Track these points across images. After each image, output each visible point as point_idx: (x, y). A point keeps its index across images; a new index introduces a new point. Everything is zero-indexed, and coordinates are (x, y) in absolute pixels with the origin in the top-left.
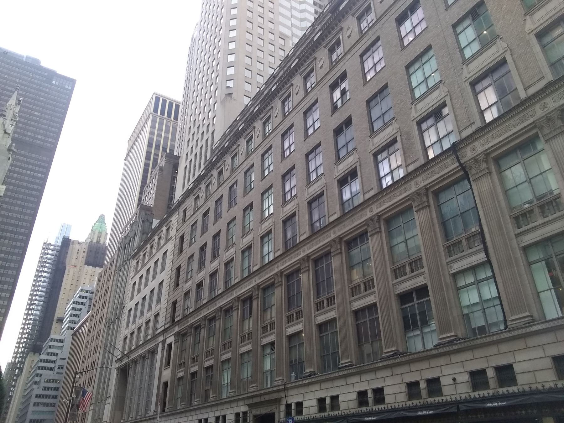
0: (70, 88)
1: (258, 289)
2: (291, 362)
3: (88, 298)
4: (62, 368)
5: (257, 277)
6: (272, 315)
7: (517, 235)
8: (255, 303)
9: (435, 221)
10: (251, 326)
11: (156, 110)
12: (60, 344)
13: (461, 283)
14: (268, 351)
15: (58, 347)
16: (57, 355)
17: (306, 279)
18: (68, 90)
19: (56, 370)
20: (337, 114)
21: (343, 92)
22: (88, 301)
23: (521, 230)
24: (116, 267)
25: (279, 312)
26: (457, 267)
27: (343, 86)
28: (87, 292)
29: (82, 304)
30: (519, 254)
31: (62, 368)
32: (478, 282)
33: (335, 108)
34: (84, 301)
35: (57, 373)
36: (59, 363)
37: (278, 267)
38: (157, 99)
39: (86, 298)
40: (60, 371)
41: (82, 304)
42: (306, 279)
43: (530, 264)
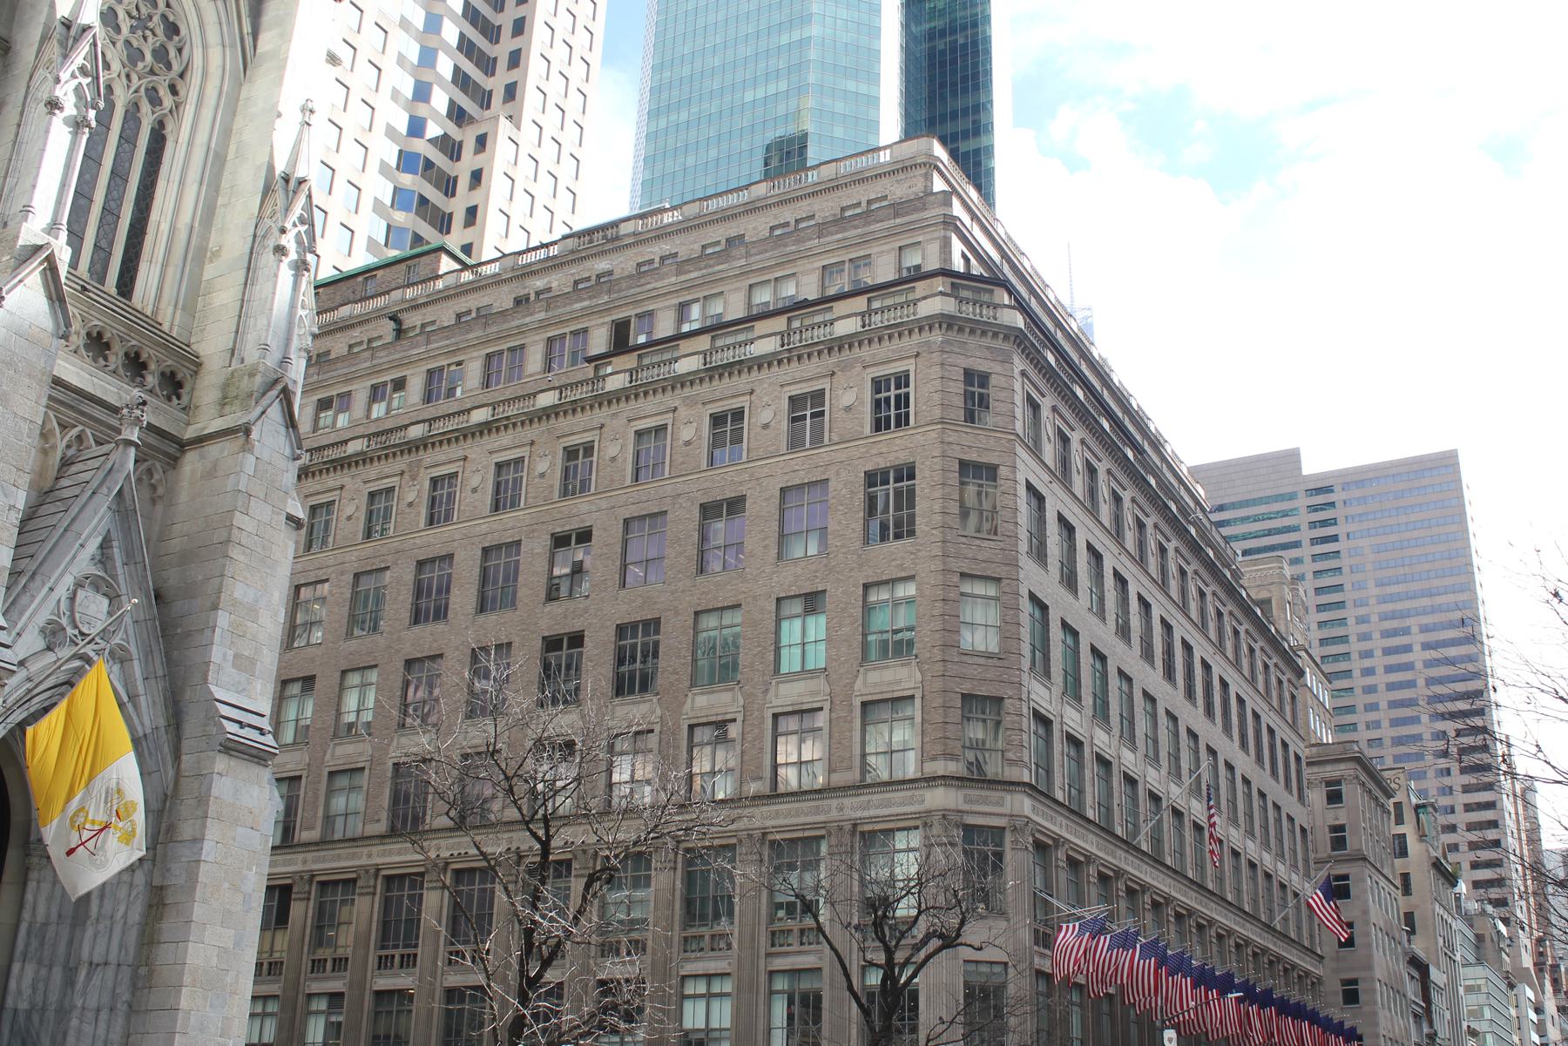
1: (311, 880)
2: (376, 1037)
5: (309, 856)
6: (346, 940)
7: (768, 955)
8: (297, 909)
9: (678, 894)
10: (277, 947)
13: (689, 990)
14: (323, 1005)
17: (434, 904)
20: (554, 608)
21: (578, 569)
23: (774, 950)
25: (362, 941)
26: (689, 968)
27: (579, 556)
30: (763, 978)
32: (709, 996)
33: (552, 595)
37: (370, 856)
42: (434, 904)
43: (771, 993)
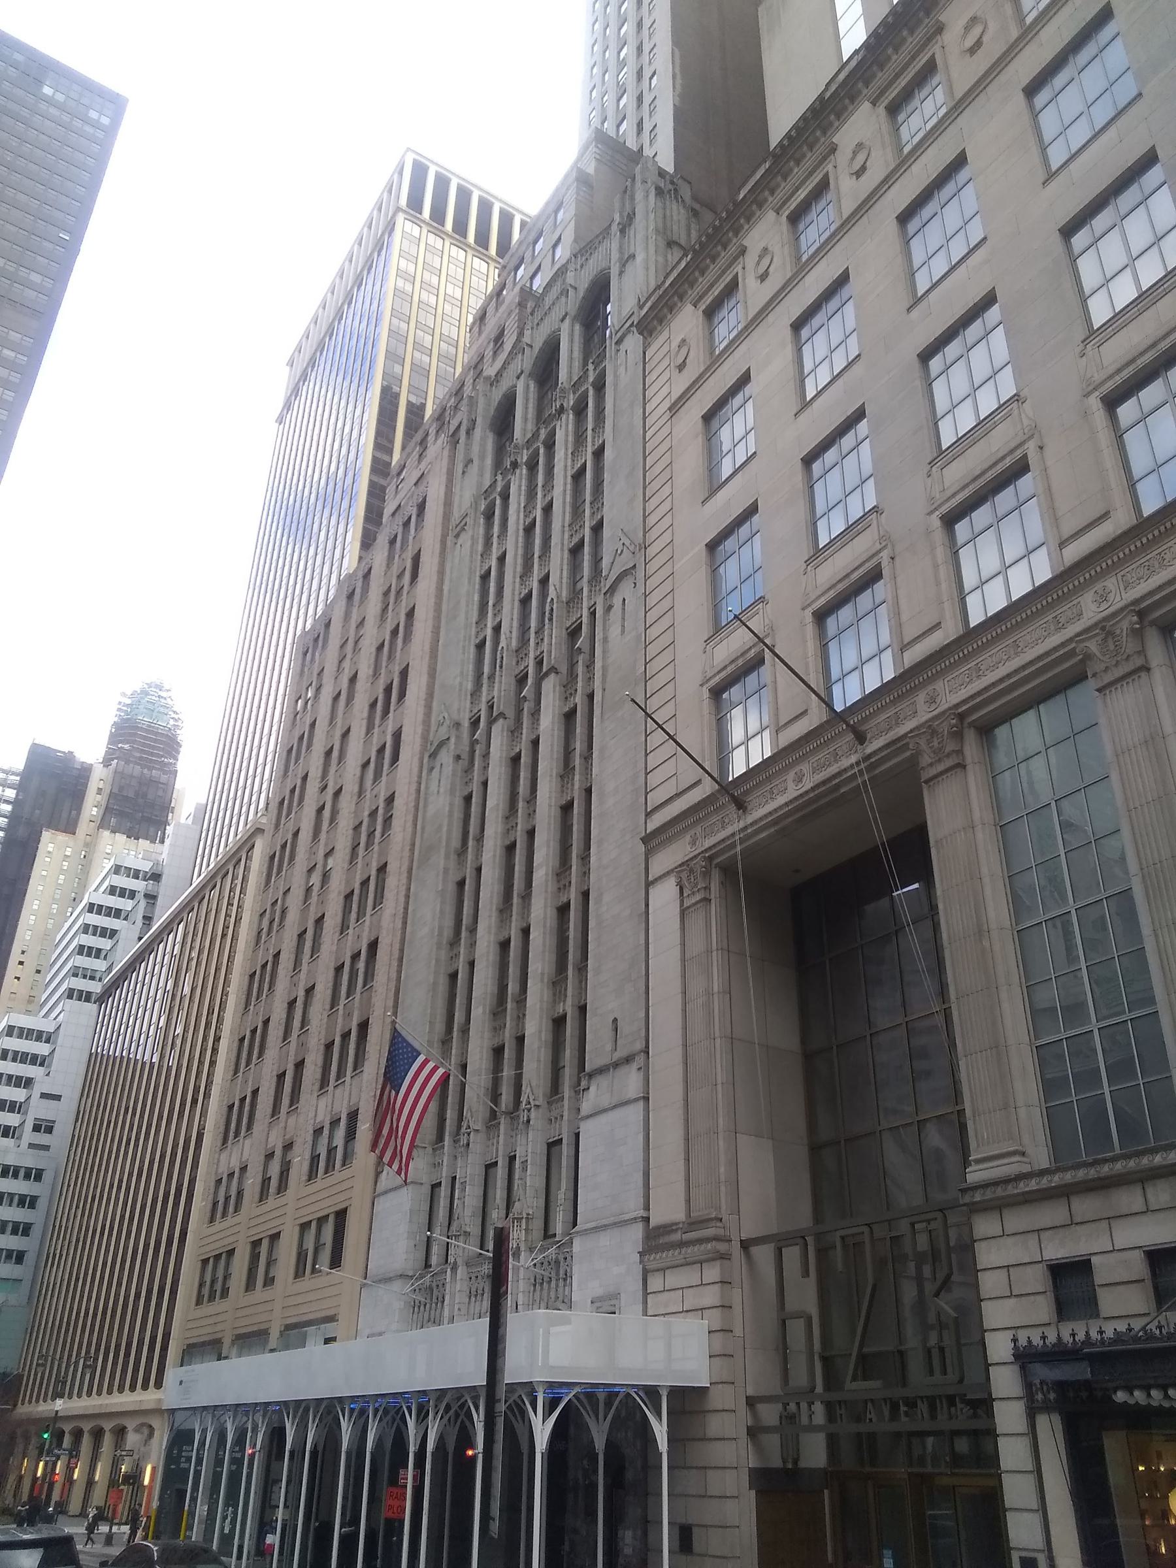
0: (105, 121)
3: (140, 896)
4: (49, 1130)
11: (415, 203)
12: (42, 1049)
15: (34, 1060)
16: (28, 1083)
18: (96, 125)
19: (28, 1136)
22: (143, 903)
24: (447, 516)
28: (136, 874)
29: (118, 913)
31: (49, 1130)
34: (126, 904)
35: (31, 1146)
36: (39, 1110)
38: (420, 171)
39: (132, 894)
40: (42, 1138)
41: (118, 913)
